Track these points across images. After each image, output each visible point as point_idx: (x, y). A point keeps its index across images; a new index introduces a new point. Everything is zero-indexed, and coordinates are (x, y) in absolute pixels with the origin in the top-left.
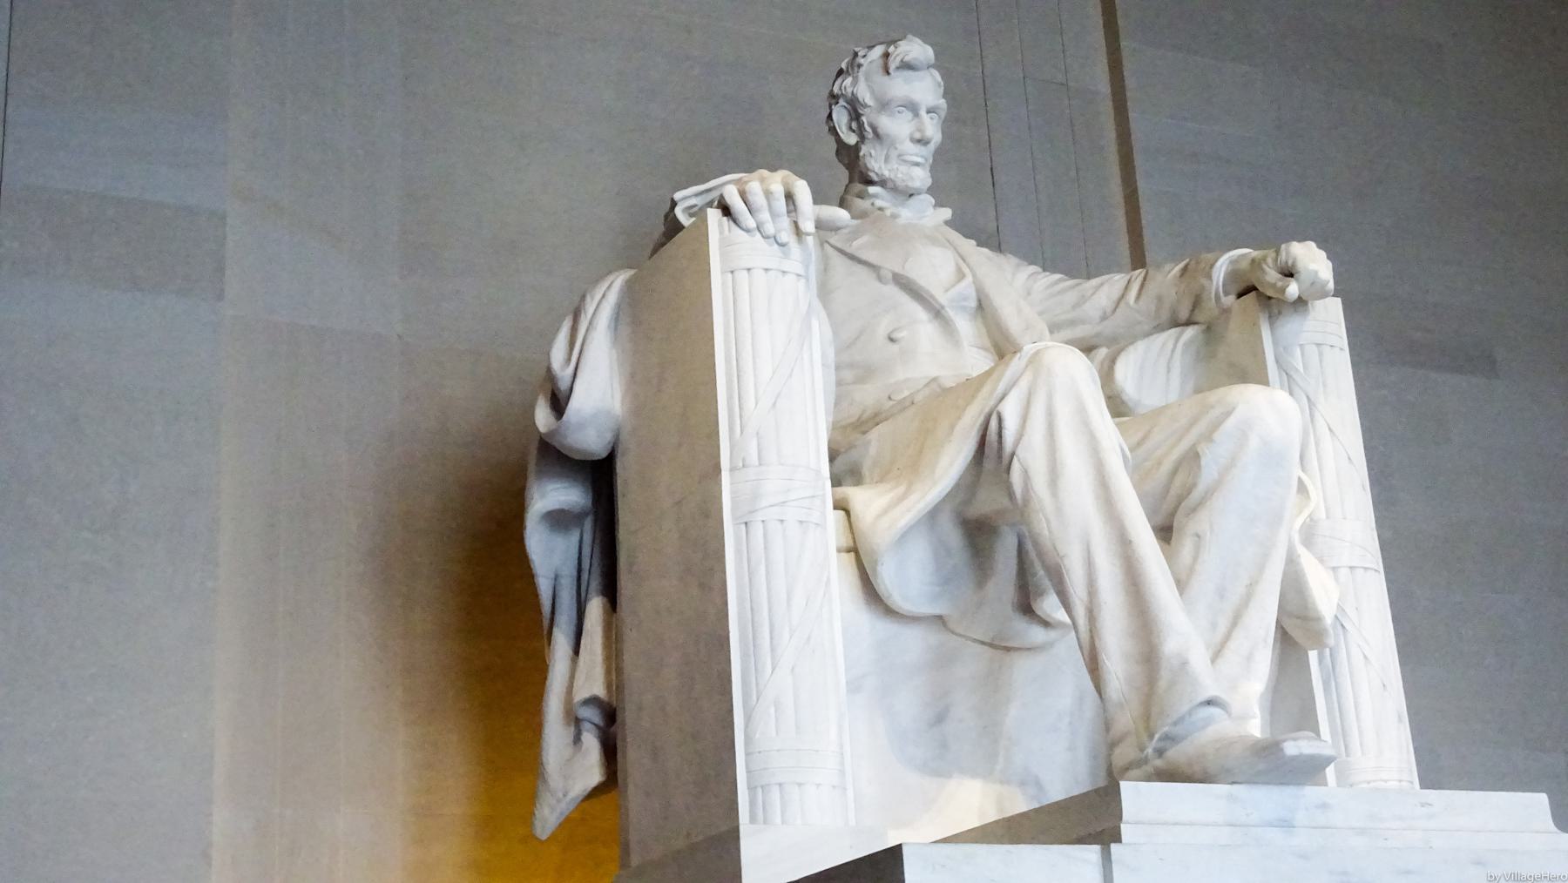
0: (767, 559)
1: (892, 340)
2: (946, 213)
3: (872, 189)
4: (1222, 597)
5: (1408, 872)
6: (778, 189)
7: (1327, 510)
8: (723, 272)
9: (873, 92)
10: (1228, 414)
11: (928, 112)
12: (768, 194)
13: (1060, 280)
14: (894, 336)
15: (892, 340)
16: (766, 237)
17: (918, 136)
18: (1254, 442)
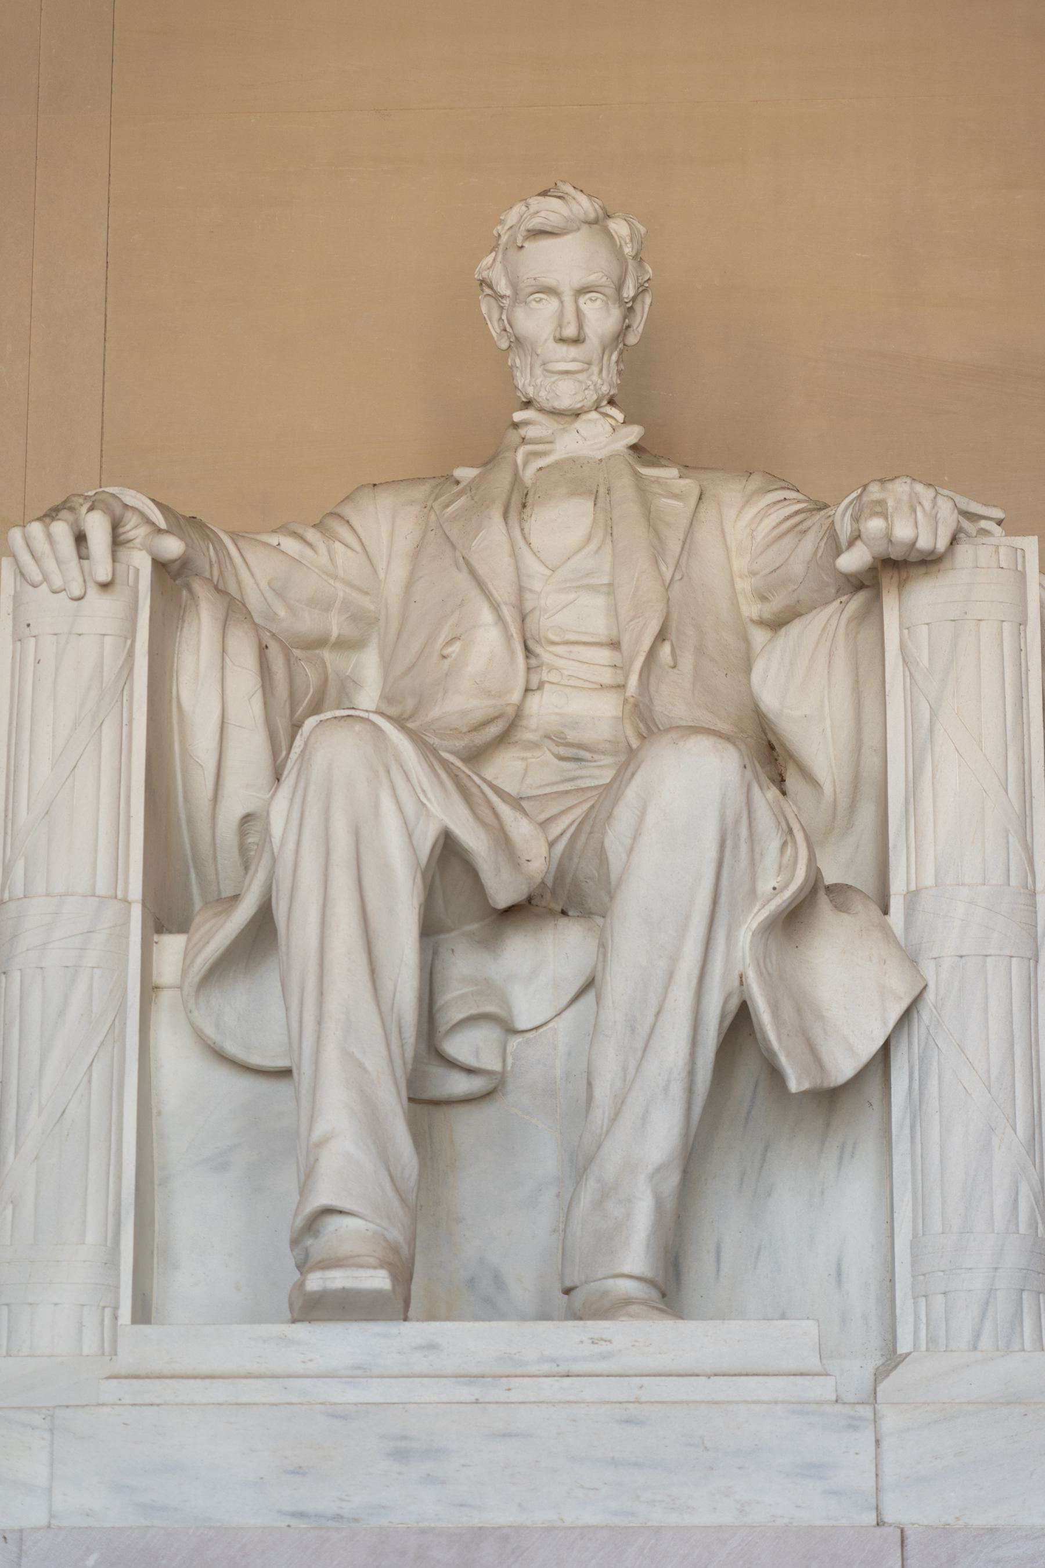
0: (21, 1021)
1: (444, 657)
2: (634, 434)
3: (518, 416)
4: (633, 1030)
5: (507, 1435)
6: (61, 530)
7: (936, 876)
8: (14, 642)
9: (507, 274)
10: (633, 774)
11: (583, 291)
12: (49, 536)
13: (797, 513)
14: (446, 652)
15: (444, 657)
16: (54, 592)
17: (558, 336)
18: (651, 818)
